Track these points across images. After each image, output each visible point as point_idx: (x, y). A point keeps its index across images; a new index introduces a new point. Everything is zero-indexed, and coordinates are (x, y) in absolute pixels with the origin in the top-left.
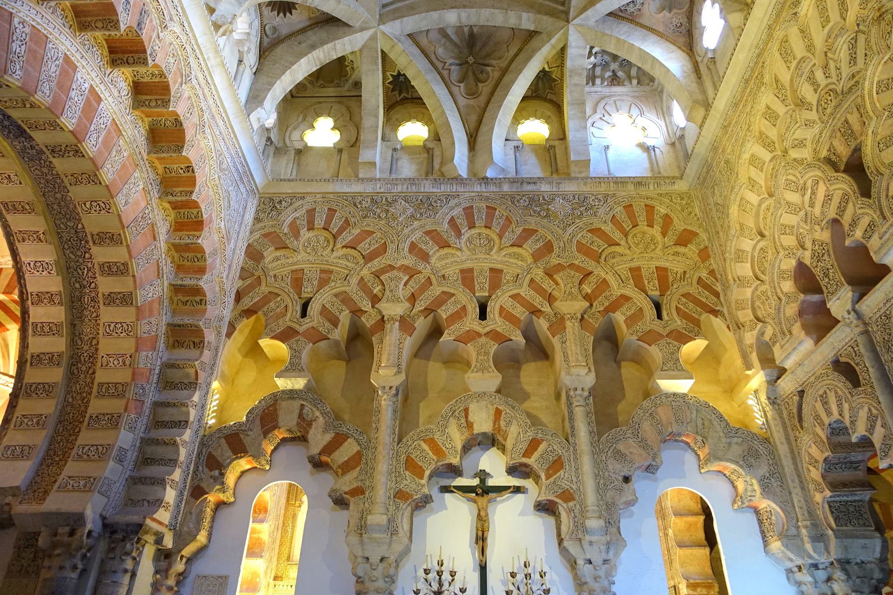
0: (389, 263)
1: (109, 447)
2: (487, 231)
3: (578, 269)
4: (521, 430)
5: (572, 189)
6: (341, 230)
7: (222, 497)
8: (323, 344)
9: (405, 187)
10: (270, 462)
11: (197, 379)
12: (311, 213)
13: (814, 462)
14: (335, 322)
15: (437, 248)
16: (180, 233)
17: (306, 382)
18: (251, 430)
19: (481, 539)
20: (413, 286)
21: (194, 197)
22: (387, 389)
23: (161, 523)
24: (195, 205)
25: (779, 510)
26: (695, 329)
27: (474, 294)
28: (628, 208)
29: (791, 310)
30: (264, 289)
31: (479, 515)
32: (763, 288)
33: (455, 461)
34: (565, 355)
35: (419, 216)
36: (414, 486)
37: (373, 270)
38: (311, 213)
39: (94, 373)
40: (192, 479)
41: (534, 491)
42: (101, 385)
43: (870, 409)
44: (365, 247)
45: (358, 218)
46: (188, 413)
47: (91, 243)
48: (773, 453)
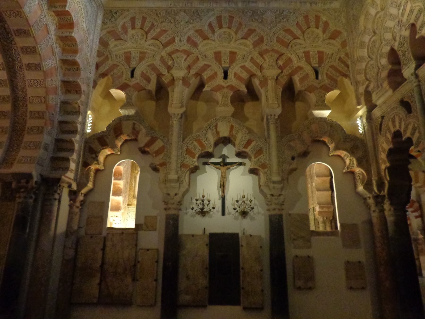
0: (176, 48)
1: (40, 143)
3: (276, 52)
7: (98, 167)
8: (143, 92)
9: (184, 4)
10: (121, 151)
11: (79, 109)
12: (133, 20)
13: (384, 150)
14: (148, 80)
17: (135, 111)
18: (109, 135)
19: (223, 186)
20: (189, 61)
21: (67, 9)
22: (176, 115)
23: (70, 179)
24: (68, 13)
26: (334, 85)
27: (221, 64)
28: (306, 17)
29: (384, 74)
30: (110, 62)
31: (222, 175)
32: (371, 62)
33: (210, 150)
34: (267, 98)
36: (191, 162)
38: (133, 20)
39: (27, 106)
40: (83, 158)
41: (249, 164)
42: (31, 112)
43: (414, 125)
44: (164, 39)
46: (76, 127)
47: (14, 35)
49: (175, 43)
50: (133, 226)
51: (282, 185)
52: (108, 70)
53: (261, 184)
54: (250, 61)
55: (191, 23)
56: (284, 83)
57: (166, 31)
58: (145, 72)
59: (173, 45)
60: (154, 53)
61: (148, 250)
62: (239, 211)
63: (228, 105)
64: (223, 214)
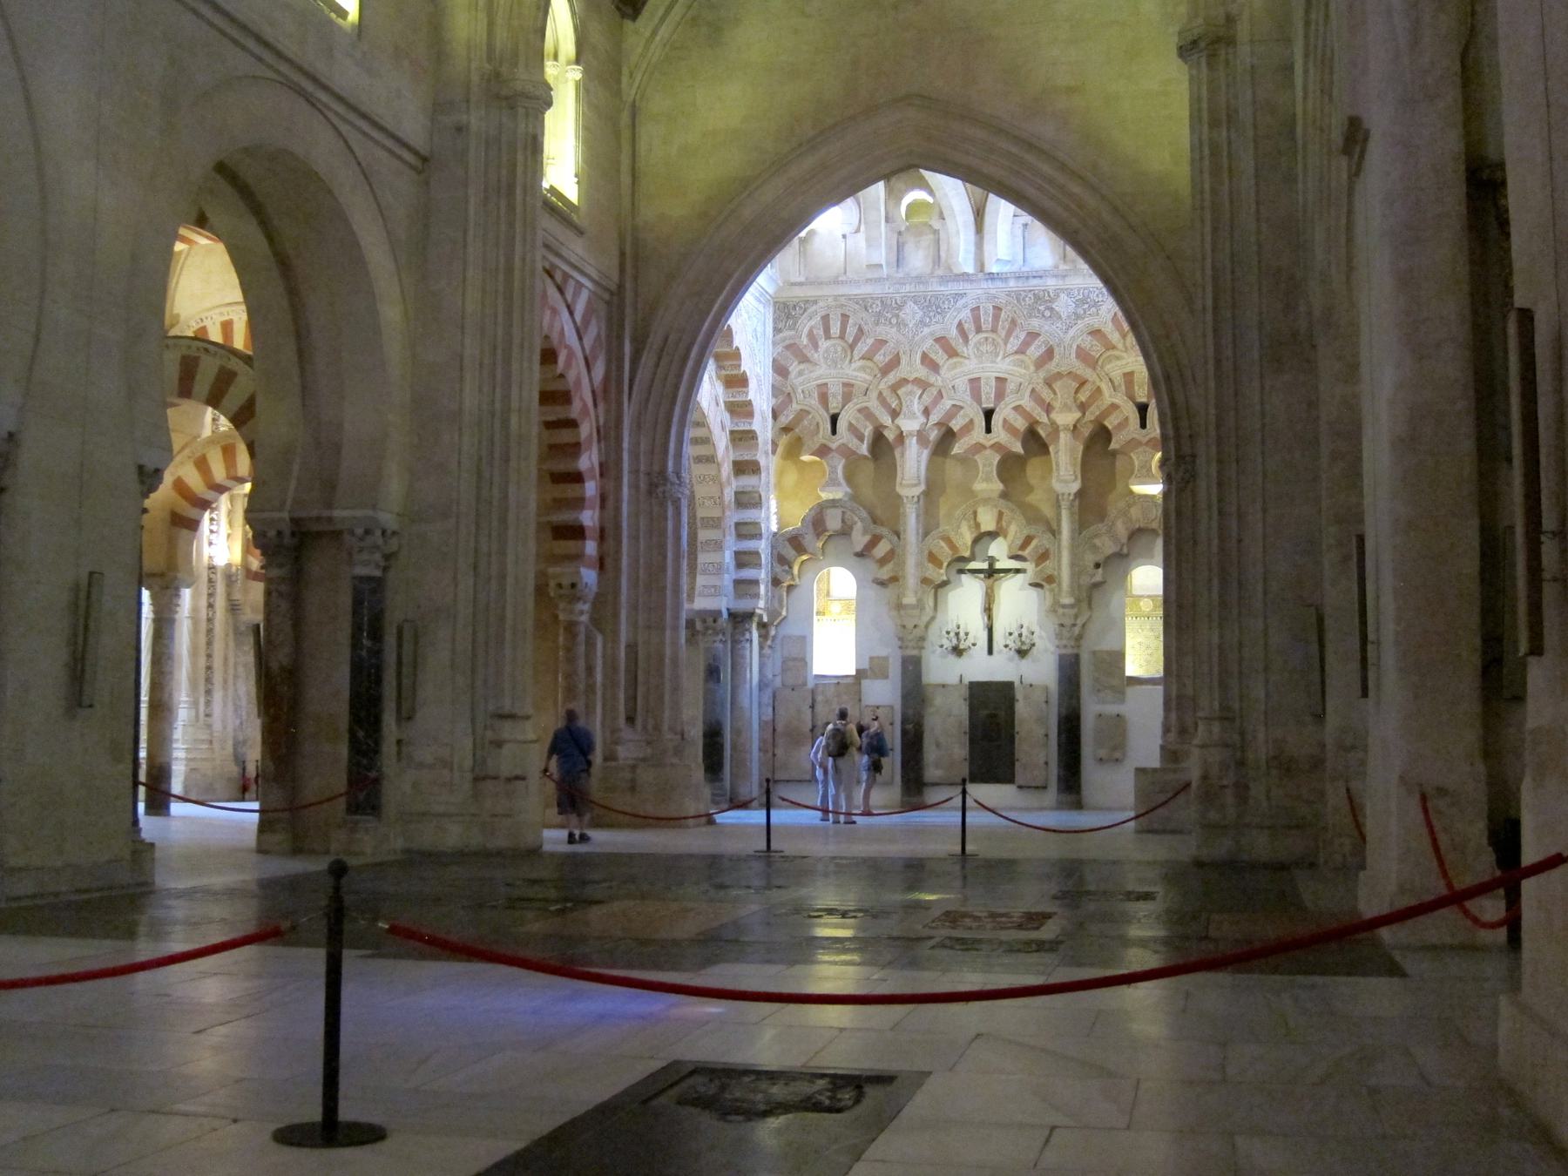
0: (903, 376)
2: (994, 336)
5: (1077, 282)
6: (857, 340)
7: (792, 583)
9: (913, 285)
10: (823, 553)
12: (826, 319)
14: (861, 438)
16: (730, 390)
19: (988, 610)
20: (927, 399)
30: (795, 407)
31: (987, 593)
33: (967, 554)
38: (826, 319)
42: (702, 518)
44: (881, 358)
50: (854, 673)
51: (1076, 610)
52: (790, 422)
55: (925, 325)
56: (1087, 435)
58: (853, 422)
60: (866, 385)
61: (878, 707)
64: (990, 652)
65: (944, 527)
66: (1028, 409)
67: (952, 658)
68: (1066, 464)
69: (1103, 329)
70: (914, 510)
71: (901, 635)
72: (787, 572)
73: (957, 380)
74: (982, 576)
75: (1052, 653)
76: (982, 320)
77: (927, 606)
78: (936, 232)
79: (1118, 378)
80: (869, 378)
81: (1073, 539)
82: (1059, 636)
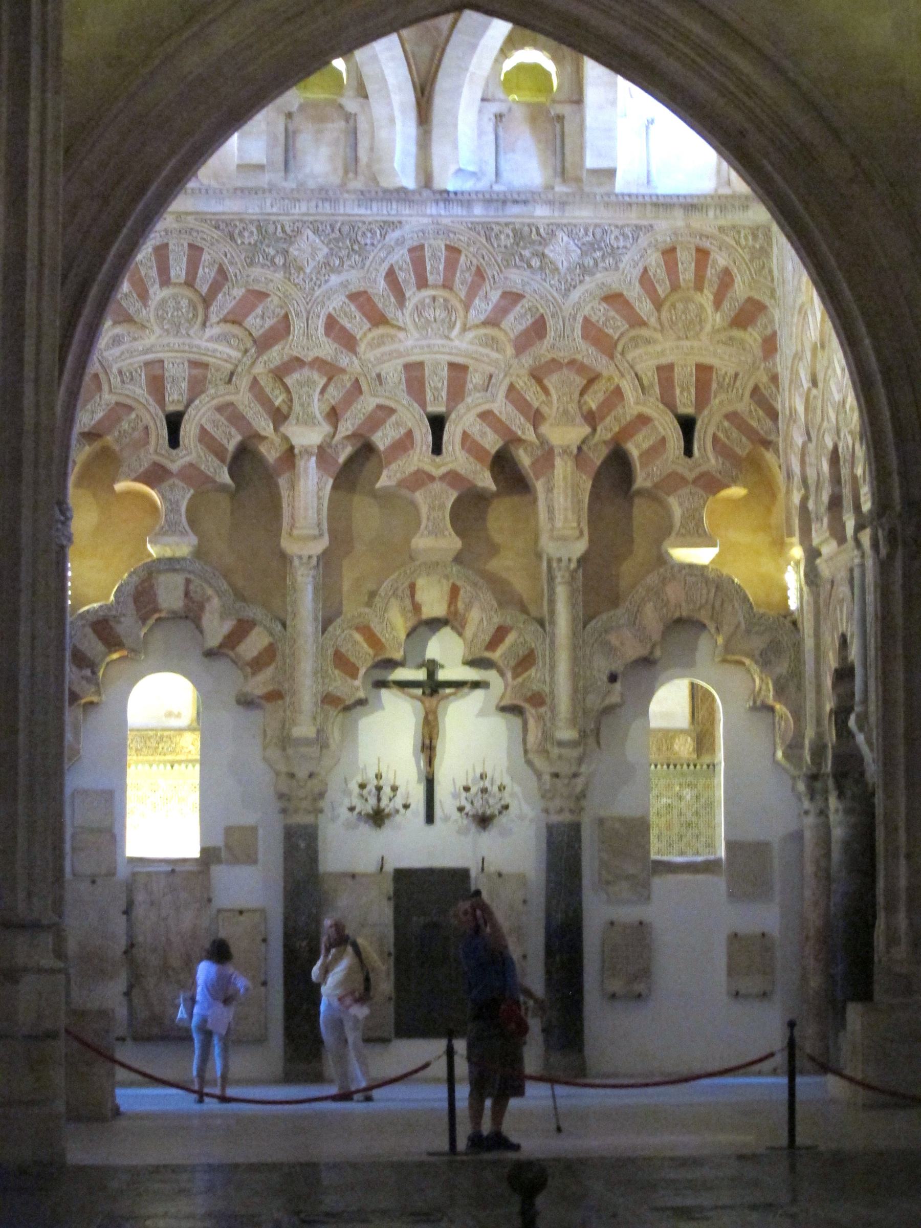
0: (295, 354)
4: (484, 616)
6: (216, 288)
9: (313, 204)
15: (368, 325)
18: (124, 615)
20: (335, 394)
22: (305, 560)
25: (789, 715)
28: (669, 253)
33: (398, 655)
35: (337, 262)
37: (272, 366)
44: (256, 323)
45: (239, 266)
48: (798, 646)
49: (291, 337)
51: (580, 750)
52: (100, 422)
53: (529, 747)
54: (507, 397)
55: (333, 270)
57: (262, 295)
58: (208, 427)
59: (286, 345)
60: (230, 367)
61: (241, 912)
62: (470, 813)
63: (446, 533)
64: (430, 818)
65: (352, 609)
66: (503, 418)
67: (366, 829)
68: (566, 509)
69: (625, 293)
70: (310, 579)
71: (285, 789)
72: (88, 680)
73: (386, 365)
74: (419, 692)
75: (531, 821)
76: (428, 268)
77: (331, 741)
78: (349, 117)
79: (650, 374)
80: (235, 354)
81: (574, 634)
82: (545, 795)
